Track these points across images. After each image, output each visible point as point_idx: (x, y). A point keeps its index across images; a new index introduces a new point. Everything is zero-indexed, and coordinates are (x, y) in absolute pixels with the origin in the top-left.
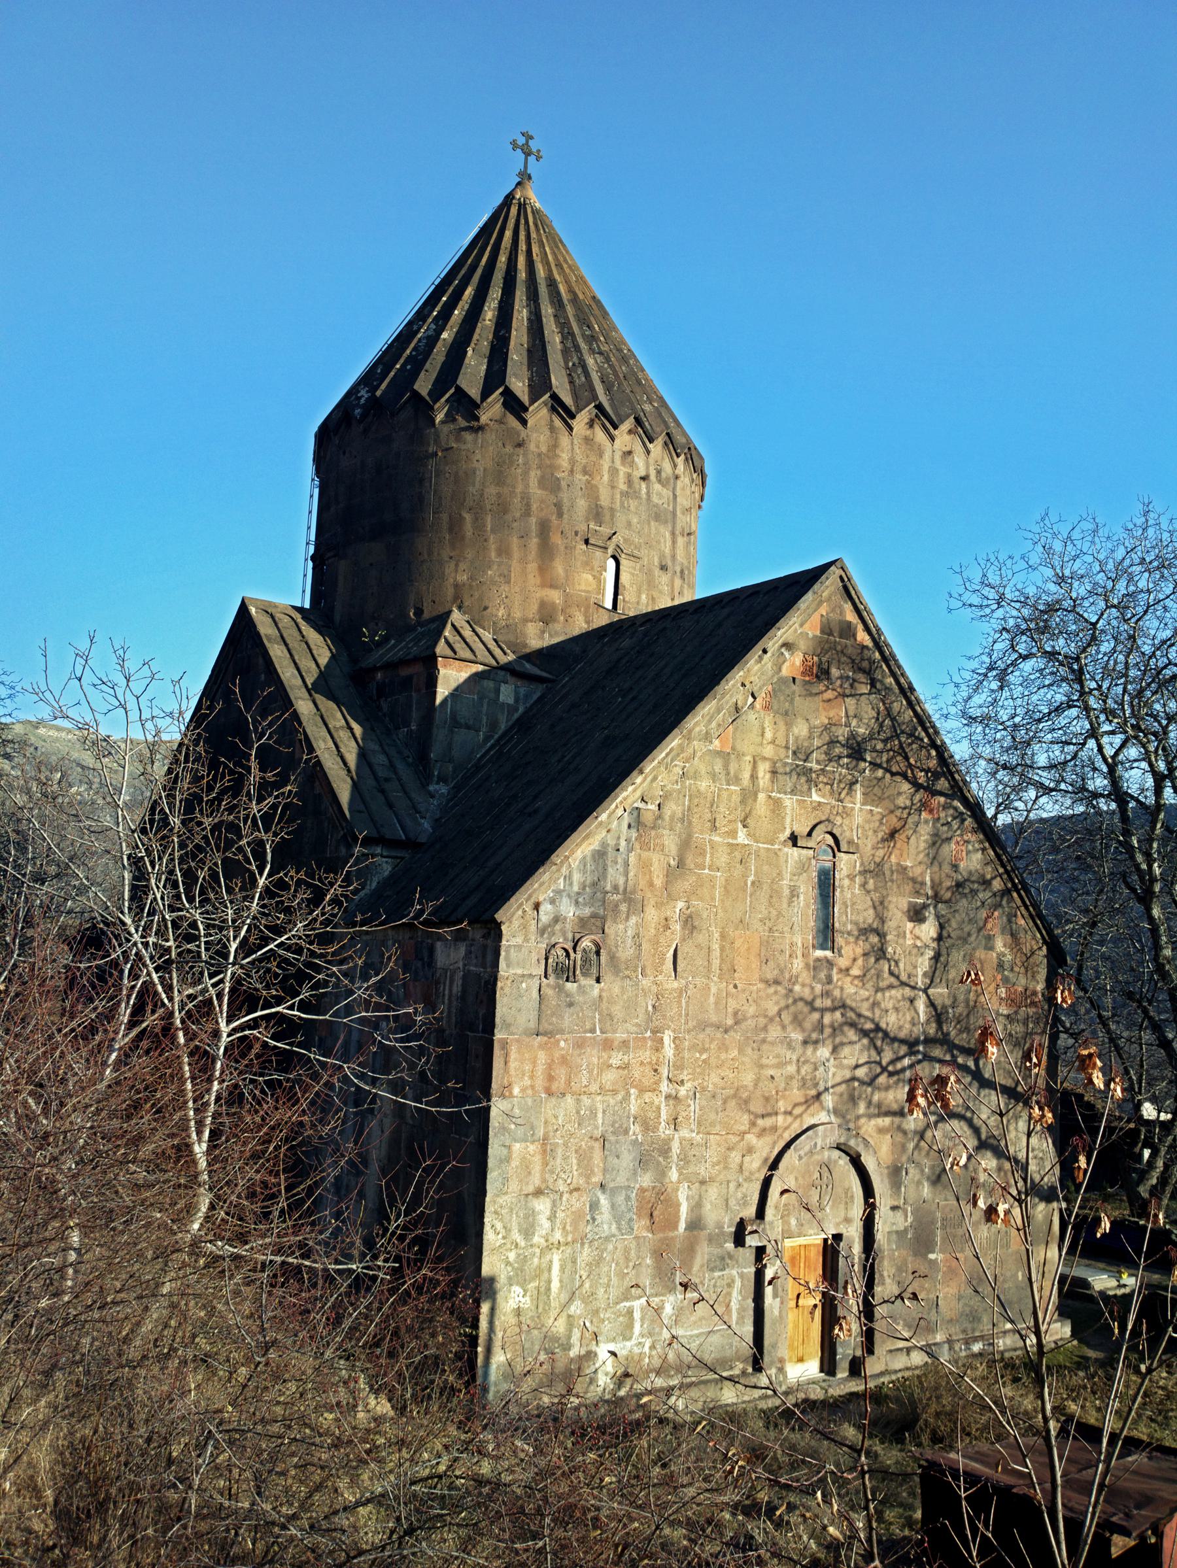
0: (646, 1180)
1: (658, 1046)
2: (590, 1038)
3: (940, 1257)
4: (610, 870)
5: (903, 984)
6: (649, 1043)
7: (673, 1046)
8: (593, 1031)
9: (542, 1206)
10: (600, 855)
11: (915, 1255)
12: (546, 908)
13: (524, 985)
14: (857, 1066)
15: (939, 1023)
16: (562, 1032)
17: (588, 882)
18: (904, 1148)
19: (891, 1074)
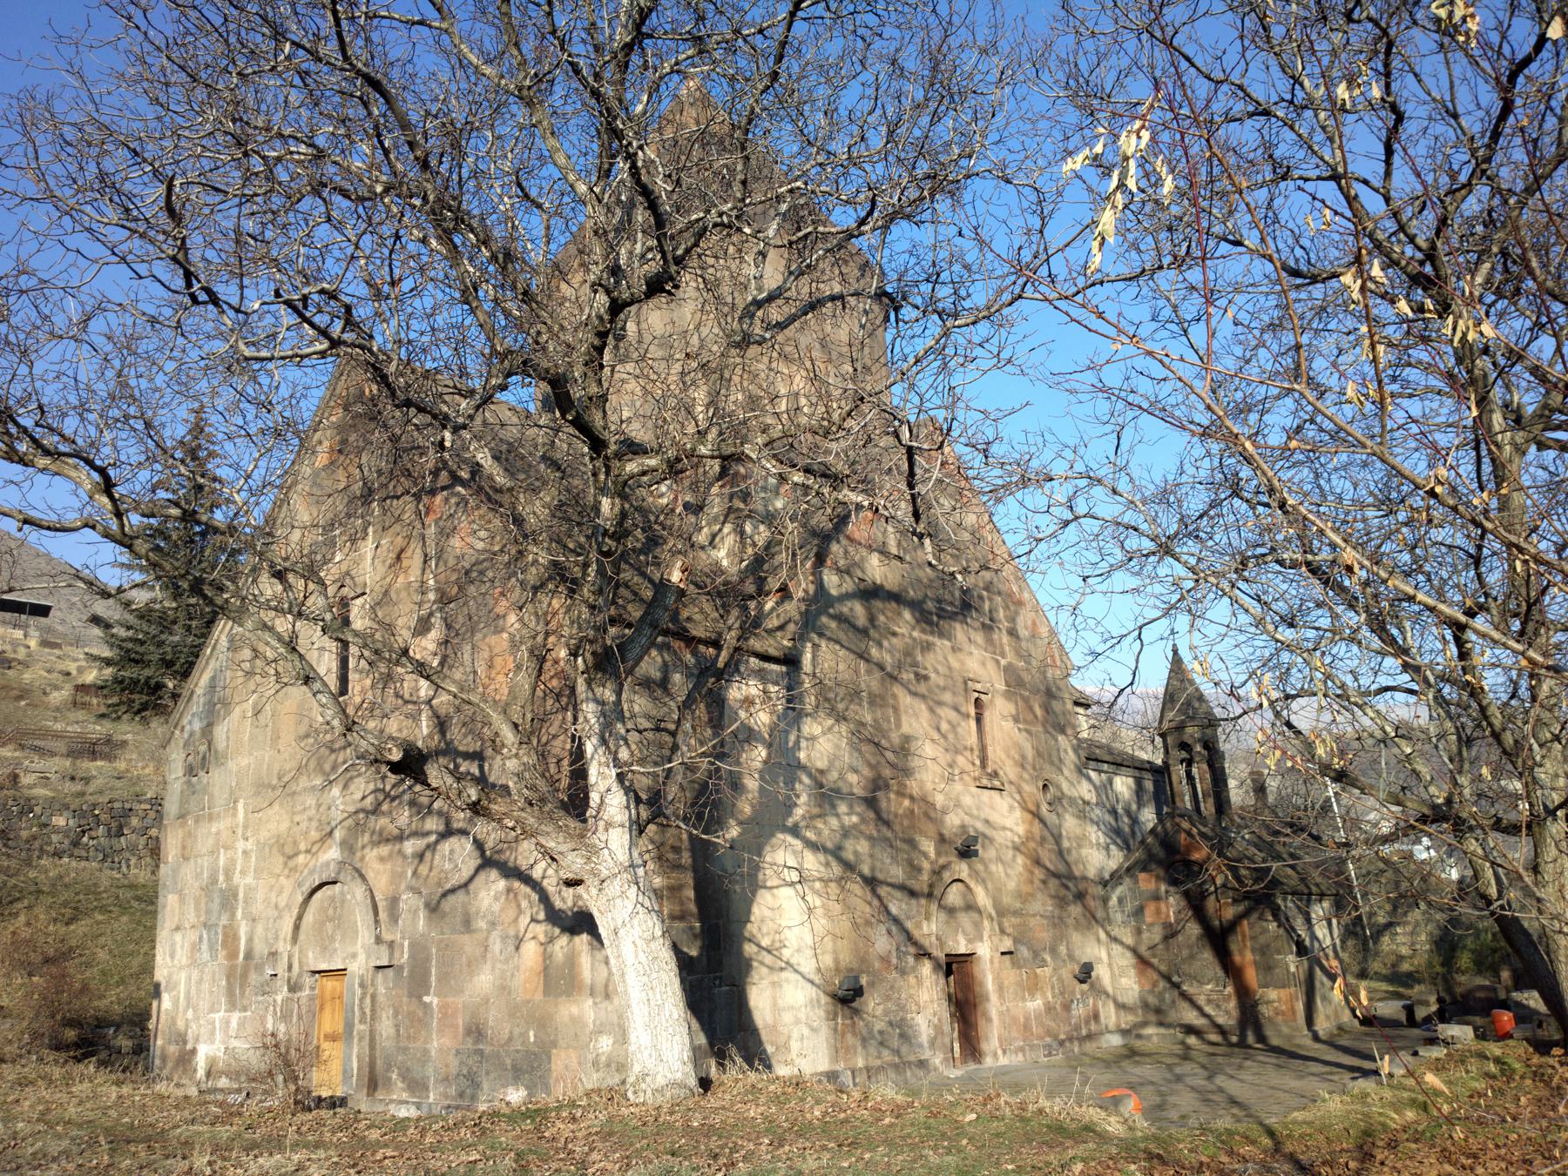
0: (224, 921)
1: (235, 808)
3: (436, 1001)
5: (407, 702)
9: (178, 937)
10: (213, 678)
11: (410, 995)
12: (188, 728)
14: (364, 798)
15: (443, 732)
18: (402, 875)
19: (393, 799)
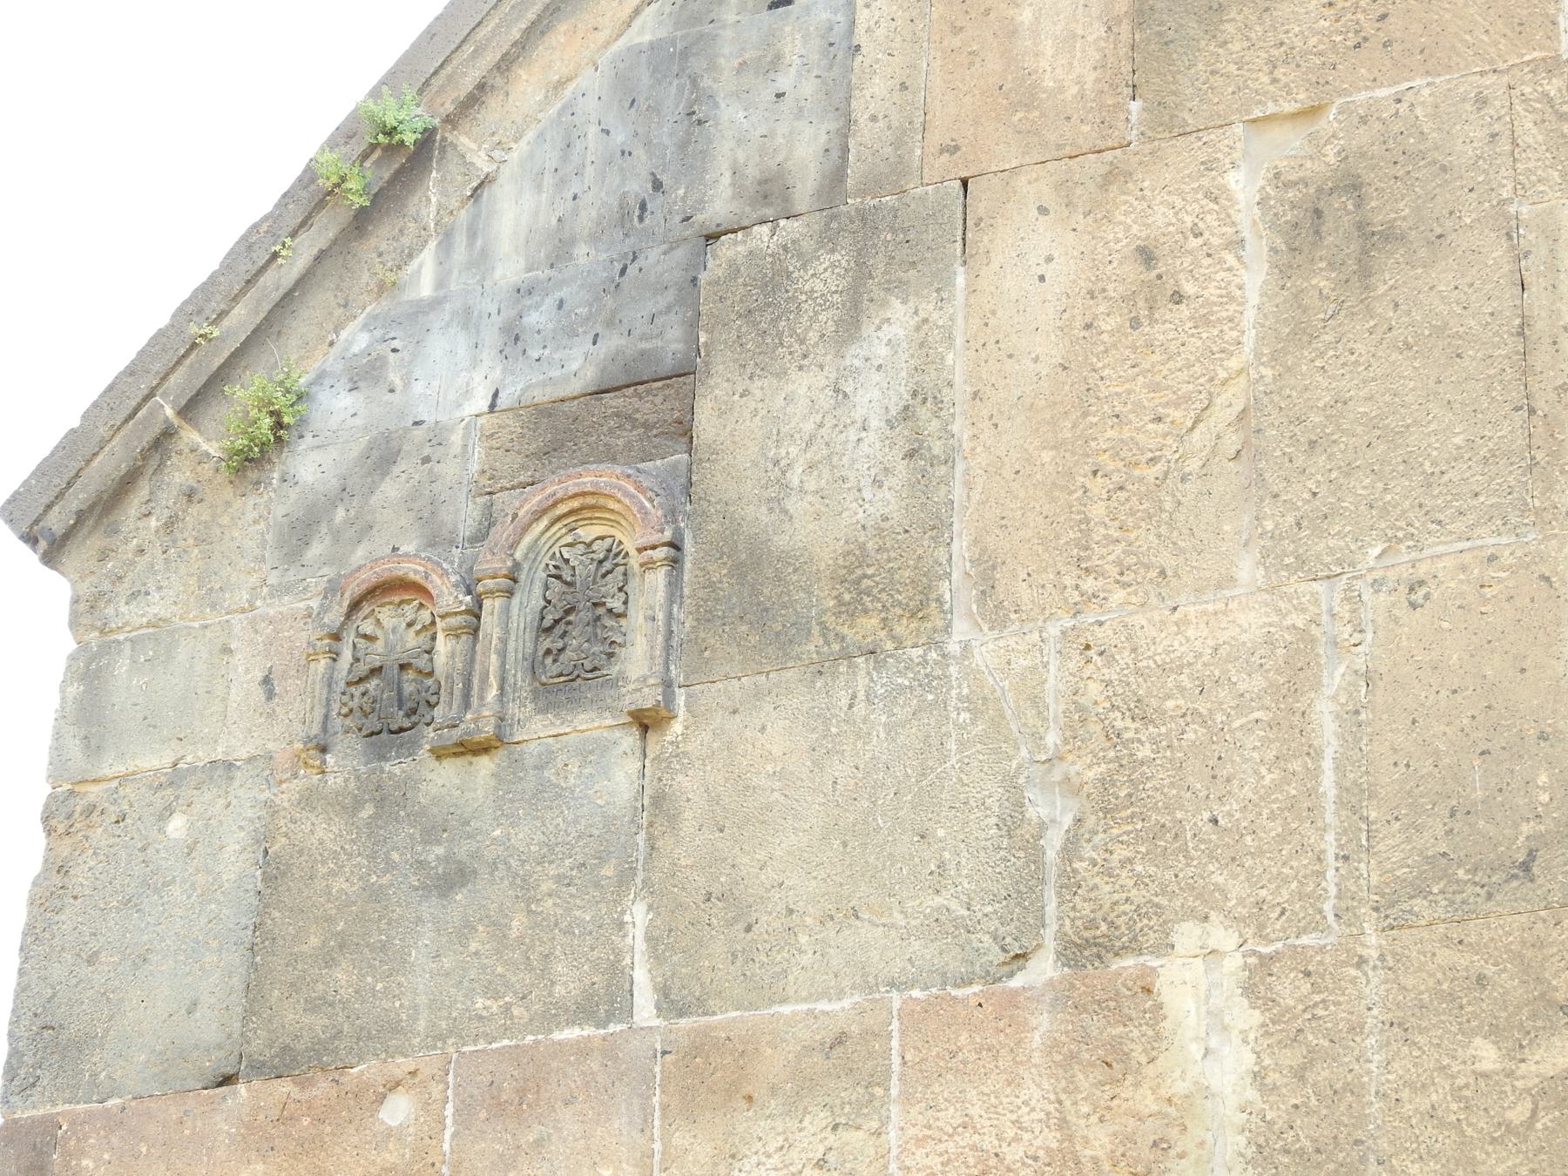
2: (582, 1050)
4: (729, 114)
6: (1042, 1025)
7: (1245, 1017)
8: (608, 1001)
13: (177, 826)
16: (386, 1035)
17: (586, 219)
